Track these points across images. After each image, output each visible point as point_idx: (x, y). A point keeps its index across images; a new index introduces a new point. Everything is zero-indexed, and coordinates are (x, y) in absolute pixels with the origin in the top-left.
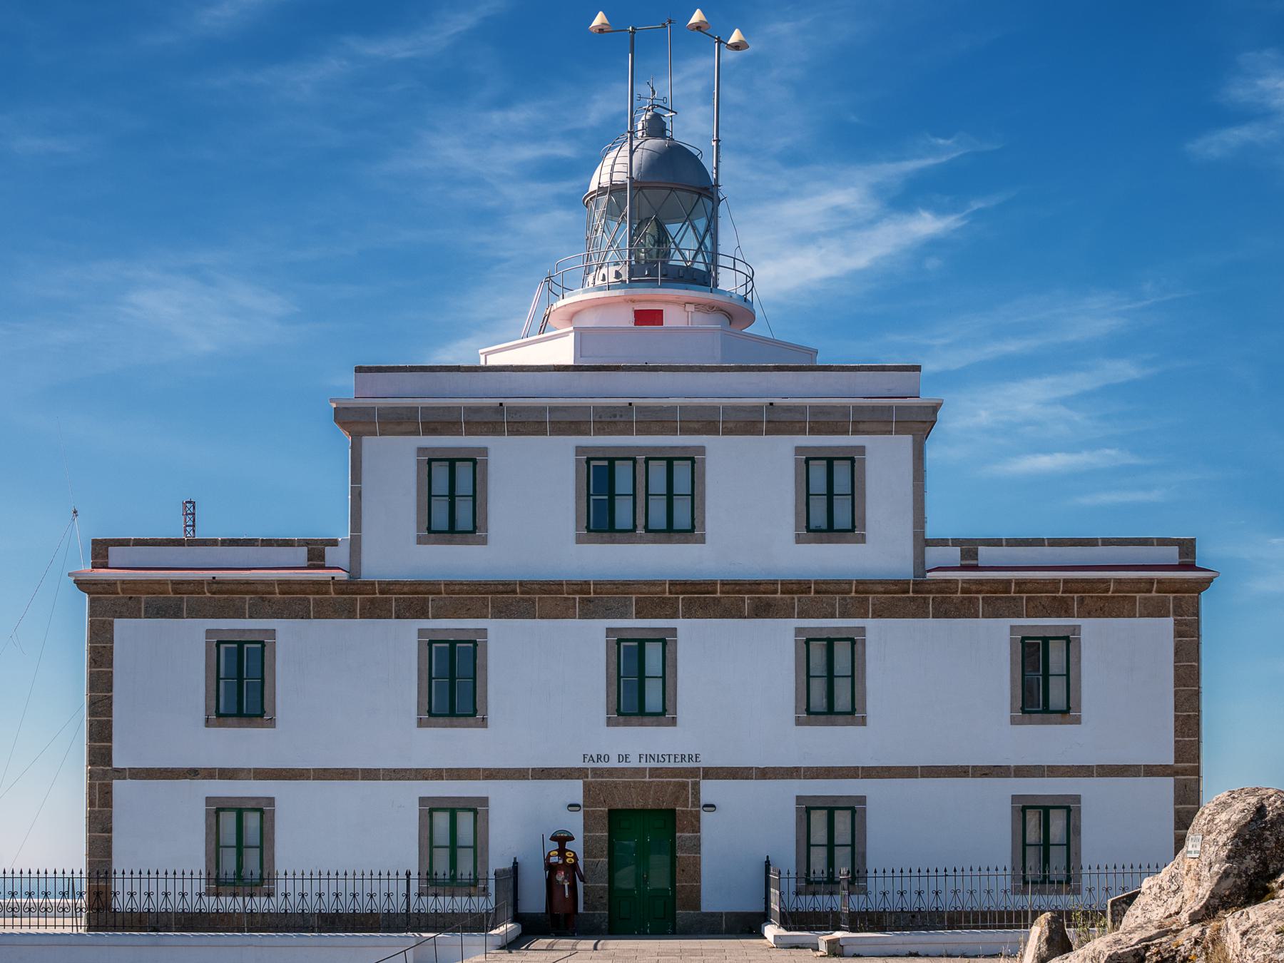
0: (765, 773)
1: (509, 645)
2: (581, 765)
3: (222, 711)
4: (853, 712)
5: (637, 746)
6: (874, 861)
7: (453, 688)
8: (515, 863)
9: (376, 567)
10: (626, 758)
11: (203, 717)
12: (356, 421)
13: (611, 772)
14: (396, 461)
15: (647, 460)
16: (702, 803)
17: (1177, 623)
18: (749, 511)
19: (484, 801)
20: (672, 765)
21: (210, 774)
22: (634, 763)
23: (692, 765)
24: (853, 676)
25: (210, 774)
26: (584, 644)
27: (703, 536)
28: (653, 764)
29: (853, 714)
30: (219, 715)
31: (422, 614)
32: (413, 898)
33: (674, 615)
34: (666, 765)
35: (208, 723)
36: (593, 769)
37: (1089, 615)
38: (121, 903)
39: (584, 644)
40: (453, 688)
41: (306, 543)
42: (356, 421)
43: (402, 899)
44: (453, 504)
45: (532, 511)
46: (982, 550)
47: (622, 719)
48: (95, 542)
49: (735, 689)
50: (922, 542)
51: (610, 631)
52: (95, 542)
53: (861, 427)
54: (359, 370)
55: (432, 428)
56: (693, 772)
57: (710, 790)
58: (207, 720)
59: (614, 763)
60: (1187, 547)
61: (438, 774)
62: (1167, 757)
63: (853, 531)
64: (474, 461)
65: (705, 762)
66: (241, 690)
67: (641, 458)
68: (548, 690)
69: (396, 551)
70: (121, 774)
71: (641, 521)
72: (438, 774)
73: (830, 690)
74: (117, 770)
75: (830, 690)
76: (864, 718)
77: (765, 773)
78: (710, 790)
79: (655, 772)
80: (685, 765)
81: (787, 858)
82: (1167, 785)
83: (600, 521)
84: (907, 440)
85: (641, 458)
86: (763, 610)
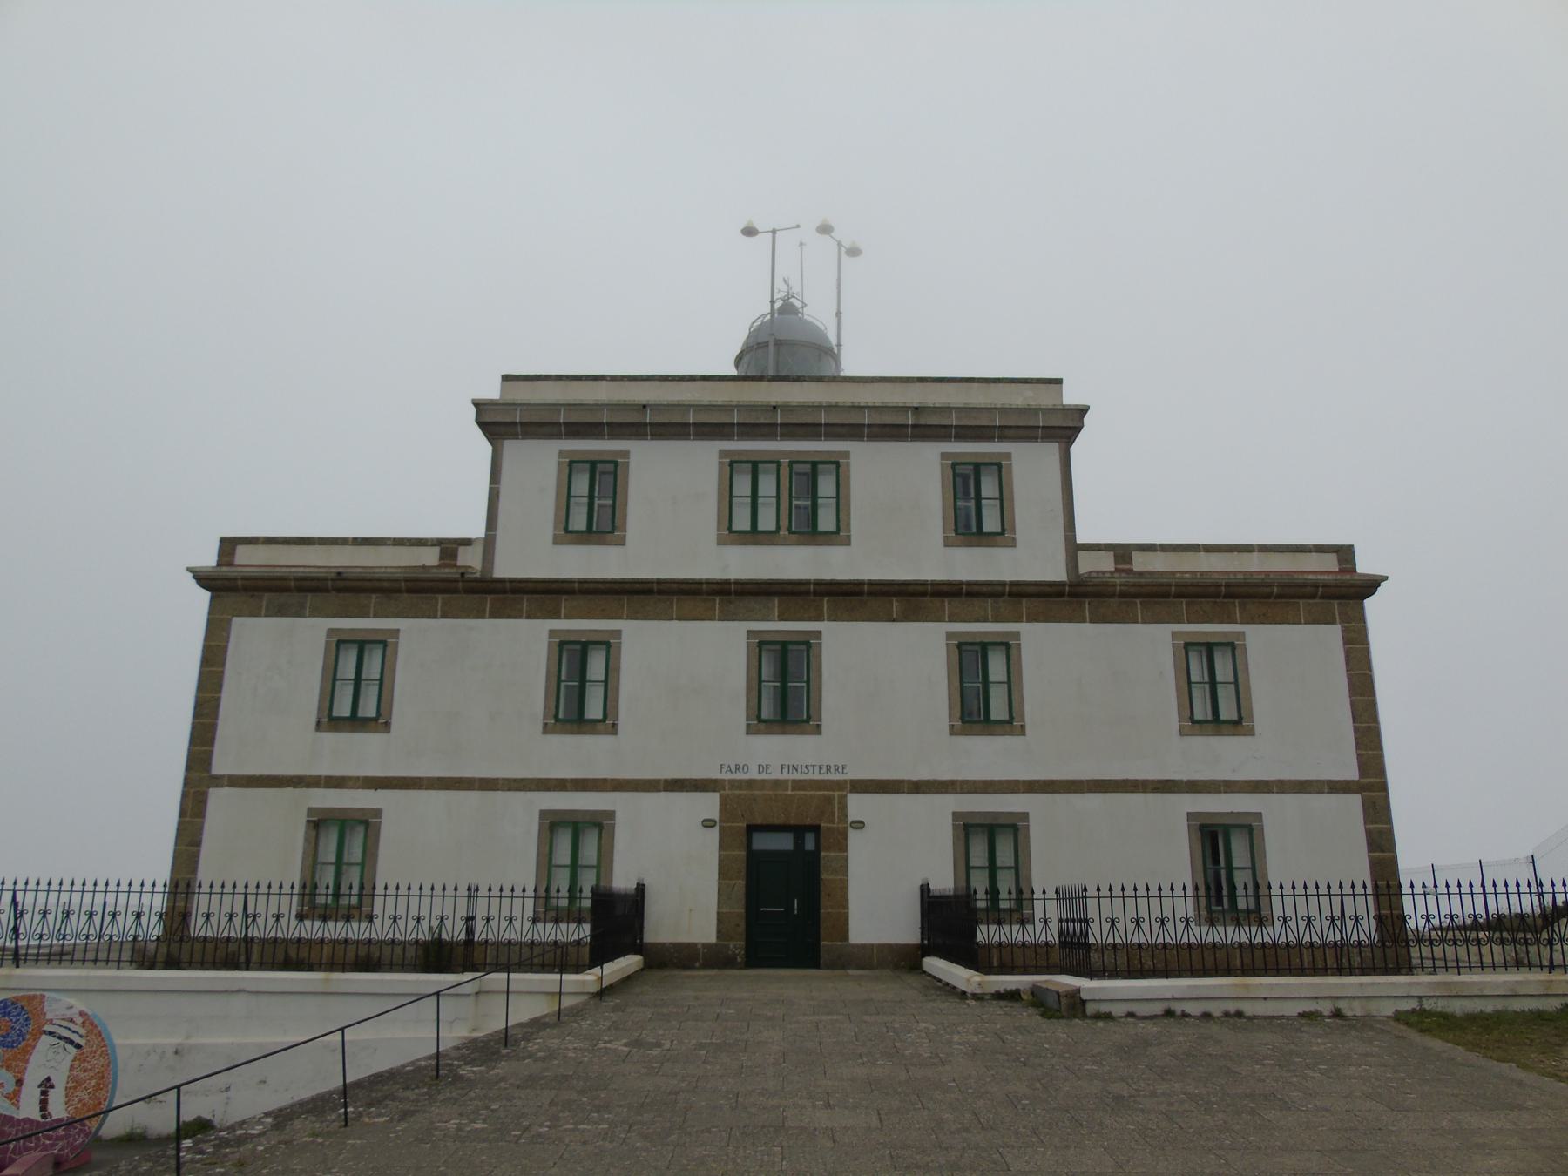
0: (917, 787)
2: (719, 776)
5: (778, 757)
8: (641, 888)
10: (764, 768)
11: (314, 719)
12: (497, 423)
13: (751, 783)
15: (791, 463)
16: (850, 819)
17: (1345, 630)
18: (894, 516)
19: (611, 815)
20: (817, 777)
22: (775, 774)
27: (849, 537)
28: (797, 776)
29: (1012, 725)
31: (555, 615)
32: (479, 925)
33: (819, 618)
36: (731, 781)
37: (1252, 620)
41: (439, 542)
42: (497, 423)
43: (460, 924)
45: (675, 514)
47: (762, 726)
48: (223, 541)
49: (885, 686)
52: (223, 541)
54: (506, 378)
55: (576, 430)
56: (839, 785)
57: (858, 806)
58: (318, 723)
59: (753, 774)
60: (1345, 554)
61: (561, 785)
62: (1349, 771)
63: (1003, 536)
65: (853, 774)
67: (785, 461)
69: (532, 555)
70: (218, 781)
71: (784, 522)
72: (561, 785)
76: (1023, 727)
77: (917, 787)
78: (858, 806)
79: (798, 784)
82: (1355, 801)
84: (1052, 449)
85: (785, 461)
86: (911, 614)
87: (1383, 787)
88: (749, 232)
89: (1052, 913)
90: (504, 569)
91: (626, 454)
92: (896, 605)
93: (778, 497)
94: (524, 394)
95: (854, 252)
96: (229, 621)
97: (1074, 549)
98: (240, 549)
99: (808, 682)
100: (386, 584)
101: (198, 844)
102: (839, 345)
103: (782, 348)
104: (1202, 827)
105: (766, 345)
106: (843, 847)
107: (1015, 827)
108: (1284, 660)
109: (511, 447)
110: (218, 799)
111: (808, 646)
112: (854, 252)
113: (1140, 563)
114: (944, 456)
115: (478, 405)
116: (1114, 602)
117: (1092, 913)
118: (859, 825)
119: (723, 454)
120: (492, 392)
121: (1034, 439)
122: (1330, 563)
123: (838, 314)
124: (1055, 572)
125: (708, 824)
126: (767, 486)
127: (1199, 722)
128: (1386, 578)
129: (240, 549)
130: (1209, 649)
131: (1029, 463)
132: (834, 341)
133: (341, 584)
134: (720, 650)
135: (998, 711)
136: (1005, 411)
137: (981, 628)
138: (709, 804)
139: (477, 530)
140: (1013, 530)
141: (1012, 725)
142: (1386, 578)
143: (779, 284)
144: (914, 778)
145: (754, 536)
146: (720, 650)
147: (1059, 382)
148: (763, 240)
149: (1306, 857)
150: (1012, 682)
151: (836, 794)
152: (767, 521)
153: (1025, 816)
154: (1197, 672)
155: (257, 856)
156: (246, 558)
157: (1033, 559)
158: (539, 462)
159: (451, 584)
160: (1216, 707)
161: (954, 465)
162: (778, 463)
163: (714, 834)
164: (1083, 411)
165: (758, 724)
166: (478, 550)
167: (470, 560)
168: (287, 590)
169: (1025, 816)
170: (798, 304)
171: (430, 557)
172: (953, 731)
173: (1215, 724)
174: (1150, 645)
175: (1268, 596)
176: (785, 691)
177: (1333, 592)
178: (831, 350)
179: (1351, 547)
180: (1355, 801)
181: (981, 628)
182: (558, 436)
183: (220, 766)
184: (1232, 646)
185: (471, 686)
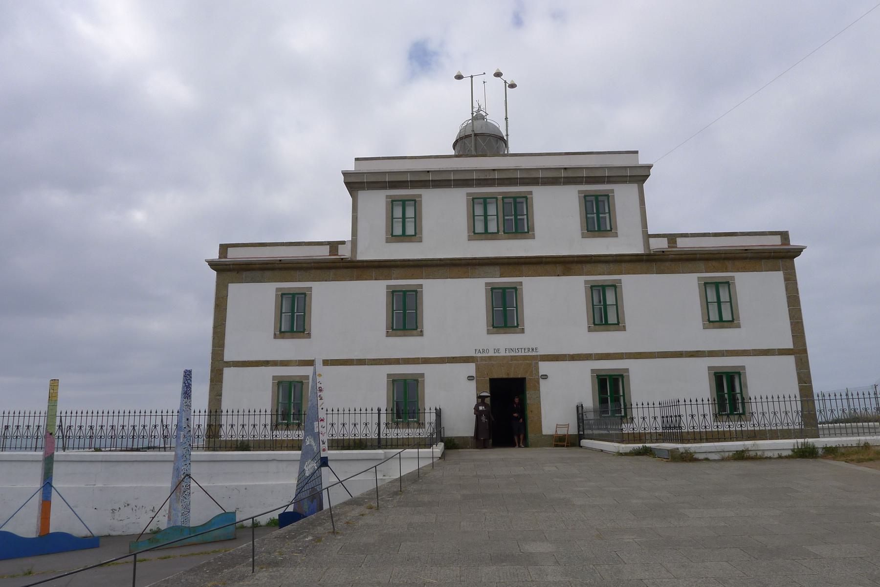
0: (573, 358)
1: (436, 293)
3: (283, 330)
4: (618, 324)
5: (504, 344)
7: (405, 316)
9: (365, 254)
13: (490, 358)
14: (376, 203)
20: (523, 354)
21: (275, 363)
22: (502, 353)
23: (534, 354)
24: (617, 305)
25: (275, 363)
28: (513, 354)
30: (281, 332)
32: (383, 426)
34: (520, 354)
35: (275, 337)
37: (738, 270)
38: (226, 433)
40: (405, 316)
41: (329, 243)
42: (356, 183)
43: (375, 427)
44: (404, 223)
45: (446, 225)
46: (679, 240)
48: (221, 246)
50: (647, 237)
51: (487, 284)
52: (221, 246)
53: (611, 179)
54: (357, 159)
55: (394, 185)
57: (544, 367)
59: (491, 354)
60: (784, 235)
62: (790, 345)
64: (415, 201)
65: (541, 352)
66: (294, 320)
67: (500, 197)
68: (455, 313)
71: (501, 229)
73: (604, 314)
74: (227, 362)
75: (604, 314)
77: (573, 358)
78: (544, 367)
79: (513, 358)
80: (530, 354)
82: (791, 359)
84: (633, 188)
87: (805, 351)
88: (459, 77)
89: (658, 414)
90: (362, 256)
91: (420, 196)
92: (559, 268)
93: (497, 215)
94: (366, 167)
95: (513, 86)
96: (227, 287)
97: (647, 237)
98: (229, 249)
99: (516, 307)
100: (305, 265)
101: (221, 395)
102: (507, 135)
103: (480, 138)
104: (715, 374)
105: (470, 136)
106: (537, 389)
108: (755, 289)
109: (362, 195)
110: (228, 372)
111: (516, 289)
112: (513, 86)
114: (580, 192)
115: (345, 174)
116: (667, 264)
117: (682, 412)
118: (545, 377)
119: (468, 194)
120: (351, 167)
121: (625, 182)
122: (776, 241)
123: (506, 118)
124: (637, 249)
125: (470, 378)
126: (492, 210)
127: (713, 322)
128: (805, 248)
129: (229, 249)
130: (717, 285)
131: (623, 196)
132: (504, 134)
133: (280, 266)
134: (473, 291)
135: (612, 319)
136: (610, 168)
137: (602, 279)
139: (347, 236)
140: (616, 229)
141: (619, 325)
142: (805, 248)
143: (476, 105)
144: (571, 353)
145: (486, 235)
146: (473, 291)
147: (637, 152)
148: (466, 81)
149: (769, 386)
150: (617, 305)
151: (534, 362)
152: (493, 228)
153: (627, 370)
154: (712, 297)
155: (250, 399)
156: (234, 255)
157: (626, 243)
158: (376, 203)
159: (338, 265)
160: (720, 312)
161: (585, 196)
162: (497, 198)
163: (473, 384)
164: (650, 167)
166: (349, 246)
167: (345, 252)
168: (253, 270)
169: (627, 370)
170: (484, 114)
172: (590, 330)
173: (721, 323)
175: (746, 258)
176: (504, 313)
177: (779, 256)
178: (502, 138)
179: (787, 232)
180: (791, 359)
181: (602, 279)
182: (384, 188)
183: (228, 356)
184: (728, 284)
185: (348, 314)
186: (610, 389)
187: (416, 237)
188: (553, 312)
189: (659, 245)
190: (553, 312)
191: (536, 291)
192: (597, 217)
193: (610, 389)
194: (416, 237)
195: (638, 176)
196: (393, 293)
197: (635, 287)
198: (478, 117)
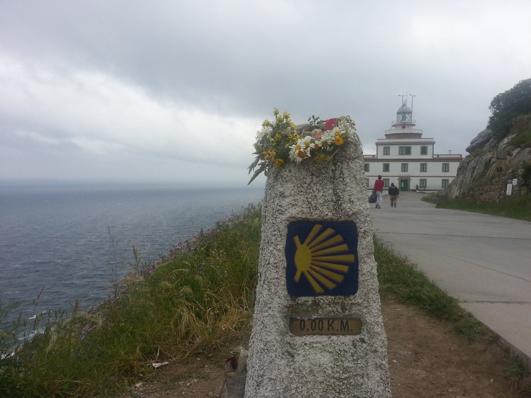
1: (392, 165)
5: (404, 174)
6: (427, 185)
7: (386, 168)
9: (379, 158)
14: (381, 148)
26: (399, 165)
29: (426, 171)
39: (399, 165)
40: (386, 168)
42: (378, 144)
44: (387, 151)
45: (394, 152)
50: (433, 155)
55: (385, 145)
57: (411, 178)
78: (411, 178)
81: (419, 185)
83: (401, 153)
84: (432, 146)
107: (426, 180)
113: (440, 156)
120: (377, 141)
122: (459, 156)
124: (431, 158)
130: (446, 164)
138: (398, 178)
145: (402, 154)
165: (402, 171)
167: (375, 157)
171: (372, 157)
174: (440, 164)
176: (405, 168)
184: (448, 164)
186: (423, 182)
187: (389, 154)
188: (414, 169)
189: (436, 156)
190: (414, 169)
191: (411, 165)
192: (424, 151)
193: (423, 182)
194: (389, 154)
195: (433, 143)
196: (384, 164)
197: (429, 164)
198: (404, 105)
